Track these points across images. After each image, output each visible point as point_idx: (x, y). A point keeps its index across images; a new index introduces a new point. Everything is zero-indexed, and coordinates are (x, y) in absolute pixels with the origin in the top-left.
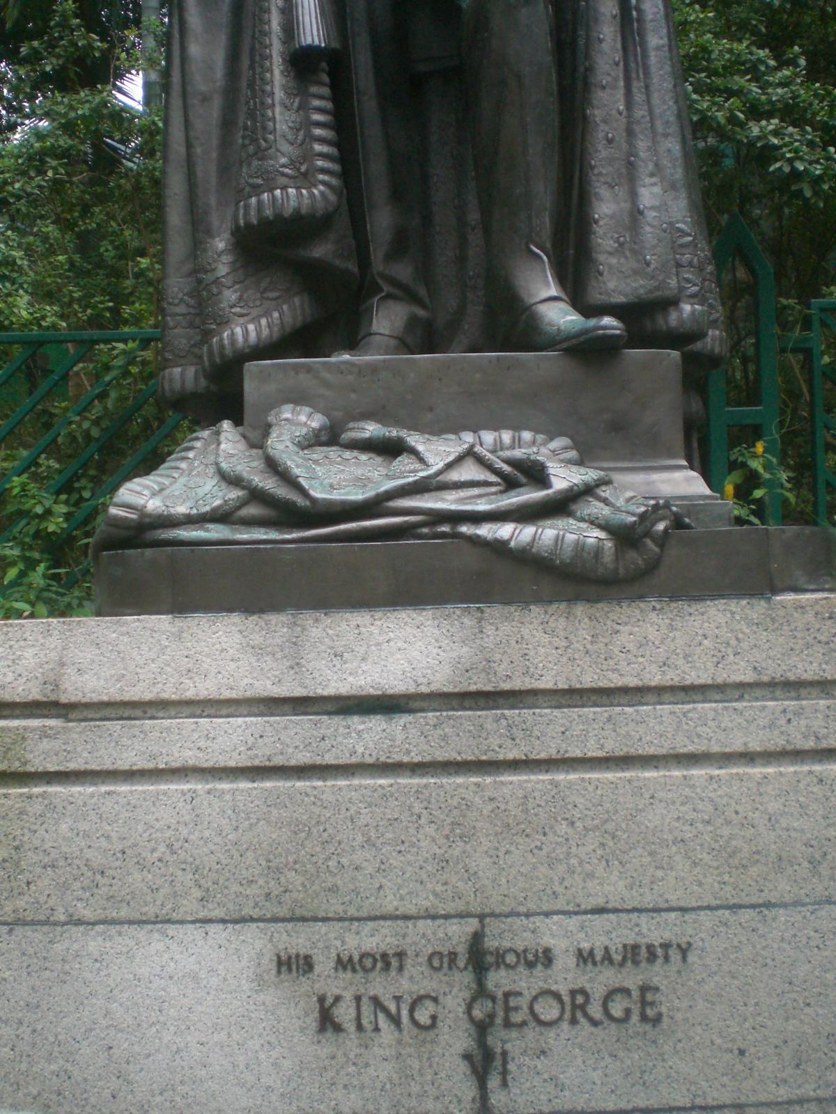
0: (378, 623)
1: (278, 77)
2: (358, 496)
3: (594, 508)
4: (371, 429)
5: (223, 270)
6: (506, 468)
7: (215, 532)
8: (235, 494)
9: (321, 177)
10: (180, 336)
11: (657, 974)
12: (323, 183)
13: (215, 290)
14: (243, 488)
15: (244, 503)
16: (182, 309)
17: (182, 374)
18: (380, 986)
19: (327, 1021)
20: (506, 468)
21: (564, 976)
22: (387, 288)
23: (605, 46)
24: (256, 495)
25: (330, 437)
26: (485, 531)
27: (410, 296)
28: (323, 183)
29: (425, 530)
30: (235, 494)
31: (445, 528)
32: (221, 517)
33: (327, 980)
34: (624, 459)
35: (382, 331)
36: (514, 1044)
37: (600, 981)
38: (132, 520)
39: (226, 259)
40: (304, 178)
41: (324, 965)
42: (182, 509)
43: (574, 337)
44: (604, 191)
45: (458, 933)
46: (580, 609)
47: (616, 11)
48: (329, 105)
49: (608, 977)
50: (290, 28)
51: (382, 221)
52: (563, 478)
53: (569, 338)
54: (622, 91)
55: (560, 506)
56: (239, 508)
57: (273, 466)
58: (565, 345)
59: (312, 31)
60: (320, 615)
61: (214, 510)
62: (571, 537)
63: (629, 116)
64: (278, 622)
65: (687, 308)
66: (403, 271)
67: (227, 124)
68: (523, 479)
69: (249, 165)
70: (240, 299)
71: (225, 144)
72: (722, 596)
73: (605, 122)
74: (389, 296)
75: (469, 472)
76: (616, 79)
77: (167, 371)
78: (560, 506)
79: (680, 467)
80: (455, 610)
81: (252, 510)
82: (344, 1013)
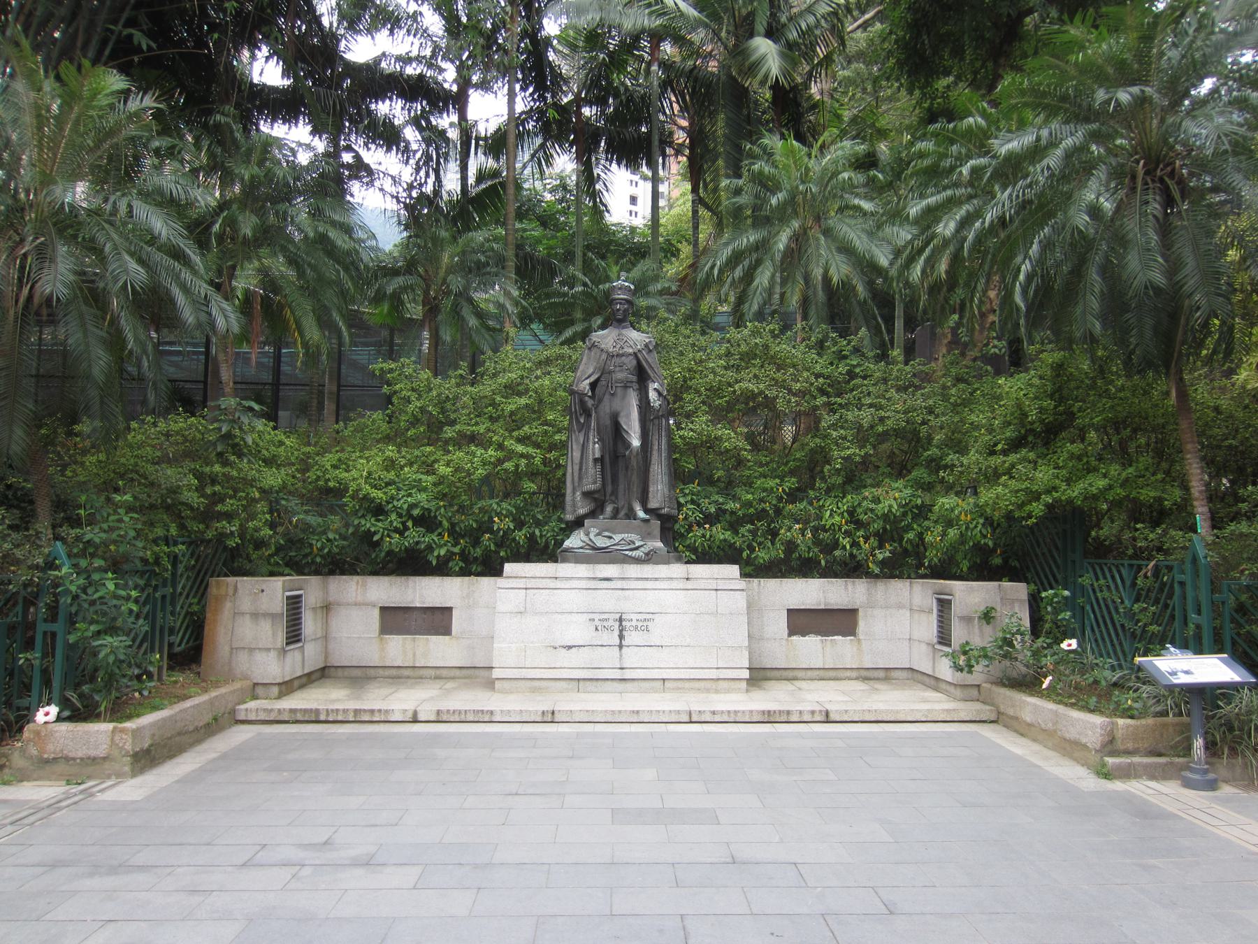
1: (591, 463)
3: (642, 549)
4: (607, 534)
7: (581, 550)
11: (649, 623)
18: (605, 624)
19: (597, 629)
21: (634, 623)
25: (598, 534)
27: (614, 503)
32: (581, 548)
33: (596, 622)
36: (624, 633)
37: (640, 624)
40: (595, 483)
41: (596, 620)
45: (618, 616)
49: (641, 624)
50: (594, 454)
51: (609, 488)
52: (638, 544)
55: (637, 548)
66: (613, 498)
67: (580, 469)
71: (580, 474)
75: (623, 542)
78: (637, 548)
82: (599, 628)
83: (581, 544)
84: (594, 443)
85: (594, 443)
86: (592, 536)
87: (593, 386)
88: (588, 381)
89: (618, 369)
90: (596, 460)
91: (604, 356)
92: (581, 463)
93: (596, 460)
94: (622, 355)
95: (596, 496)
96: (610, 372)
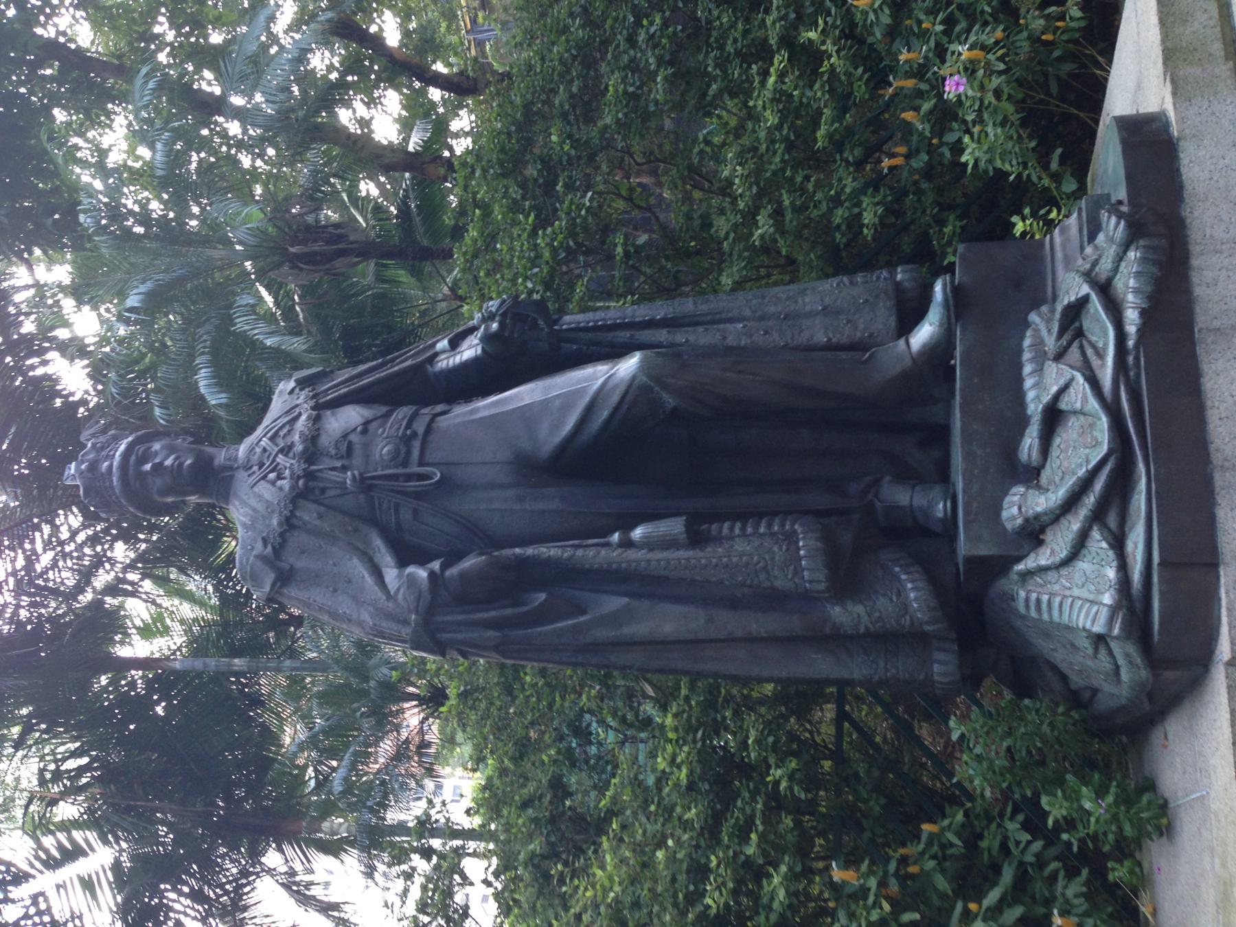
0: (1216, 404)
2: (1104, 421)
5: (859, 609)
6: (1067, 337)
8: (1096, 534)
9: (787, 527)
10: (901, 667)
12: (792, 525)
13: (877, 614)
14: (1090, 528)
15: (1104, 525)
16: (881, 664)
17: (939, 662)
20: (1067, 337)
22: (870, 496)
23: (692, 338)
24: (1098, 516)
26: (1131, 329)
28: (792, 525)
29: (1132, 374)
30: (1096, 534)
31: (1131, 359)
32: (1118, 543)
34: (1044, 279)
35: (908, 498)
38: (1124, 616)
39: (850, 607)
40: (791, 538)
42: (1111, 573)
43: (948, 311)
44: (806, 335)
46: (1195, 262)
47: (664, 332)
48: (726, 525)
50: (668, 544)
53: (949, 318)
54: (728, 326)
55: (1105, 289)
56: (1110, 530)
57: (1071, 503)
58: (953, 320)
59: (674, 526)
60: (1212, 448)
61: (1112, 546)
62: (1132, 283)
63: (748, 320)
64: (1219, 479)
65: (899, 277)
67: (734, 604)
68: (1077, 324)
69: (775, 577)
70: (884, 595)
72: (1178, 170)
73: (751, 336)
74: (876, 495)
76: (718, 330)
77: (936, 678)
78: (1105, 289)
79: (1052, 239)
80: (1200, 350)
81: (1112, 520)
83: (1098, 543)
84: (627, 544)
85: (627, 544)
86: (1042, 503)
87: (406, 555)
88: (391, 575)
89: (357, 460)
90: (696, 539)
91: (308, 514)
92: (707, 601)
93: (696, 539)
94: (312, 439)
95: (847, 538)
96: (366, 485)
